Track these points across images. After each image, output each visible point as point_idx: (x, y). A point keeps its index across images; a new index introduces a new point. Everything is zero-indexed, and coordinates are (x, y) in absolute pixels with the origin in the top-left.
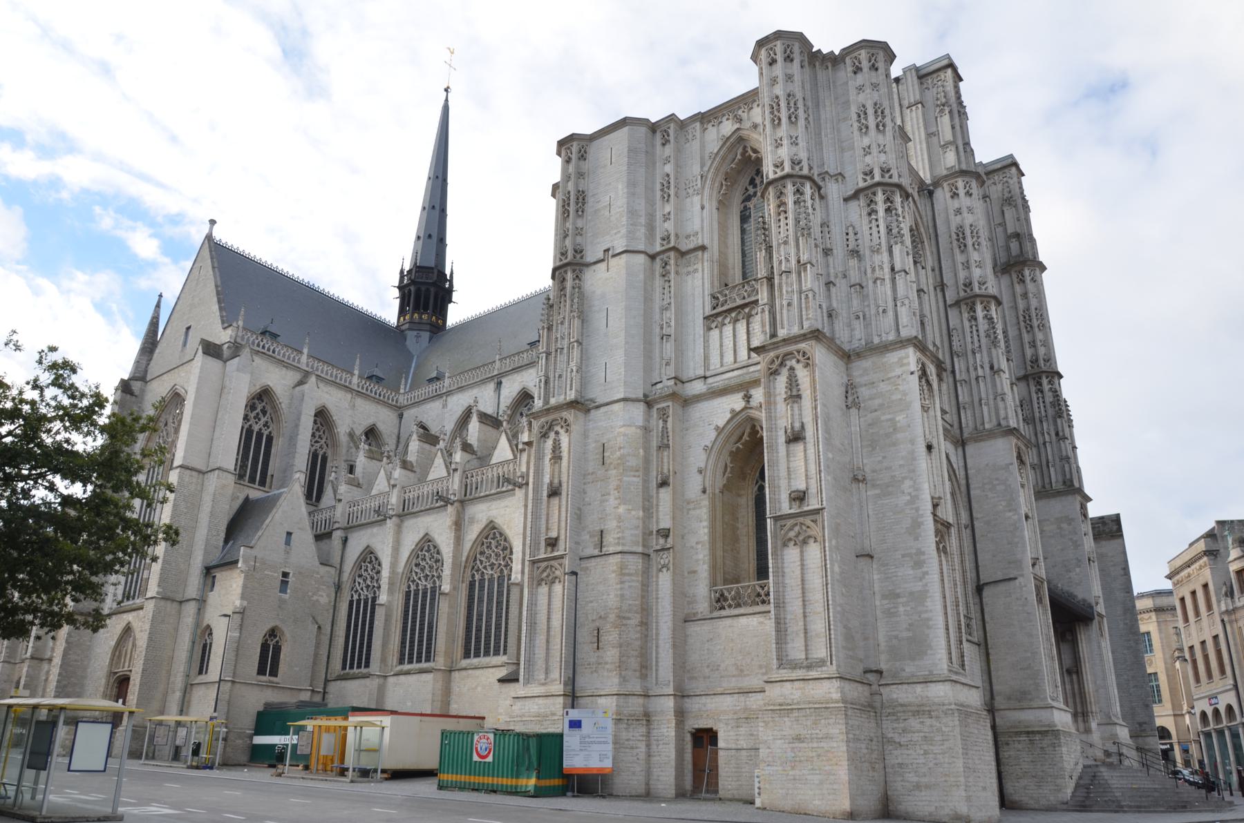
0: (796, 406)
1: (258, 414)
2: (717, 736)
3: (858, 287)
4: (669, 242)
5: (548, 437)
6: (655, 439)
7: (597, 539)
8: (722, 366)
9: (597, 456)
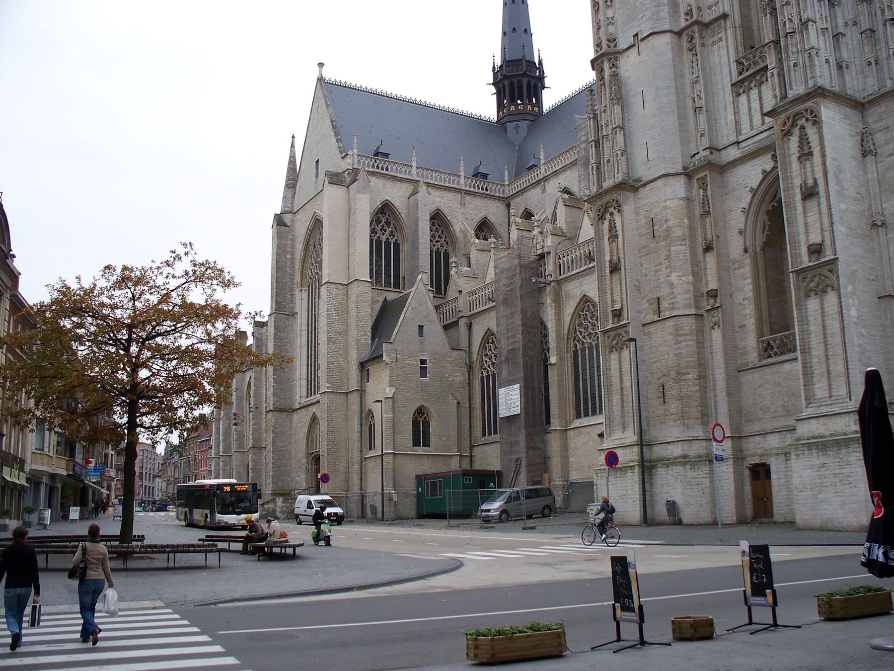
0: (808, 163)
1: (383, 226)
2: (770, 469)
3: (868, 32)
4: (692, 17)
5: (605, 218)
6: (698, 207)
7: (655, 306)
8: (752, 129)
9: (648, 231)
